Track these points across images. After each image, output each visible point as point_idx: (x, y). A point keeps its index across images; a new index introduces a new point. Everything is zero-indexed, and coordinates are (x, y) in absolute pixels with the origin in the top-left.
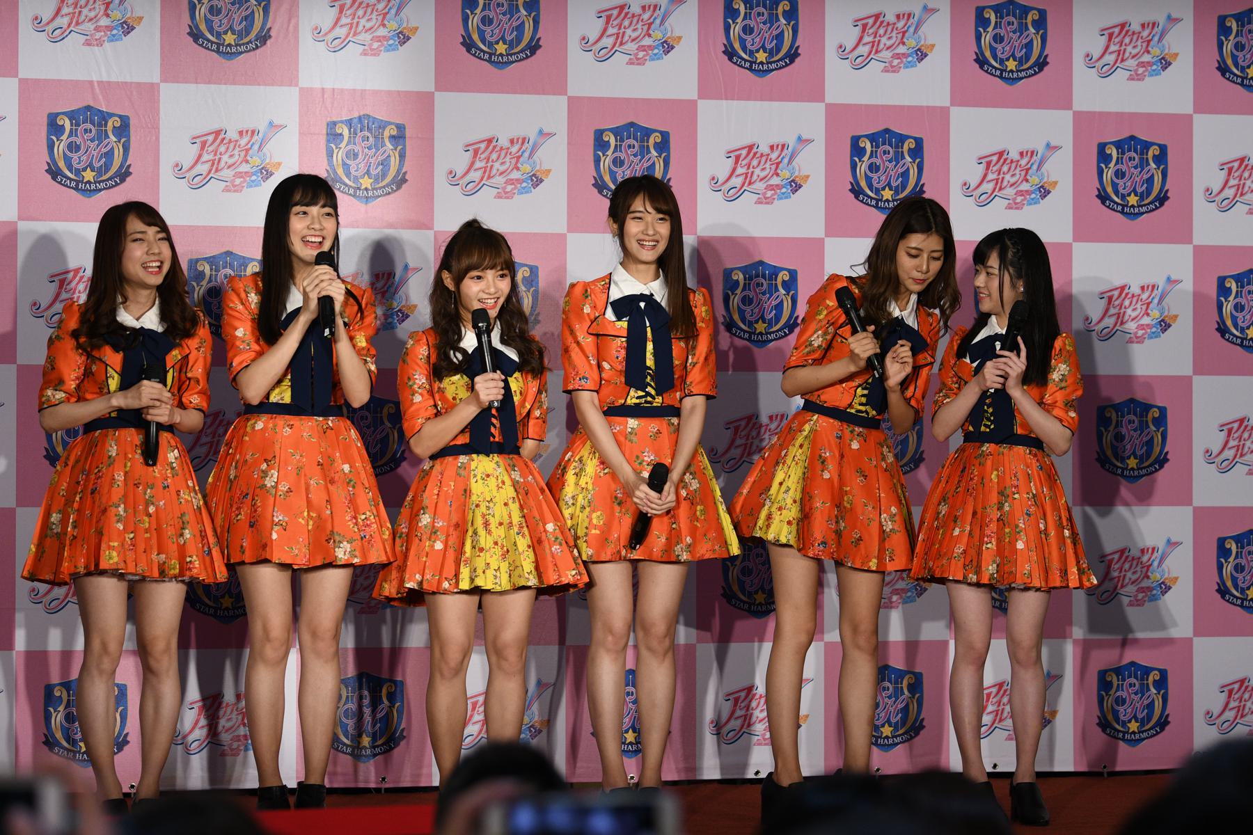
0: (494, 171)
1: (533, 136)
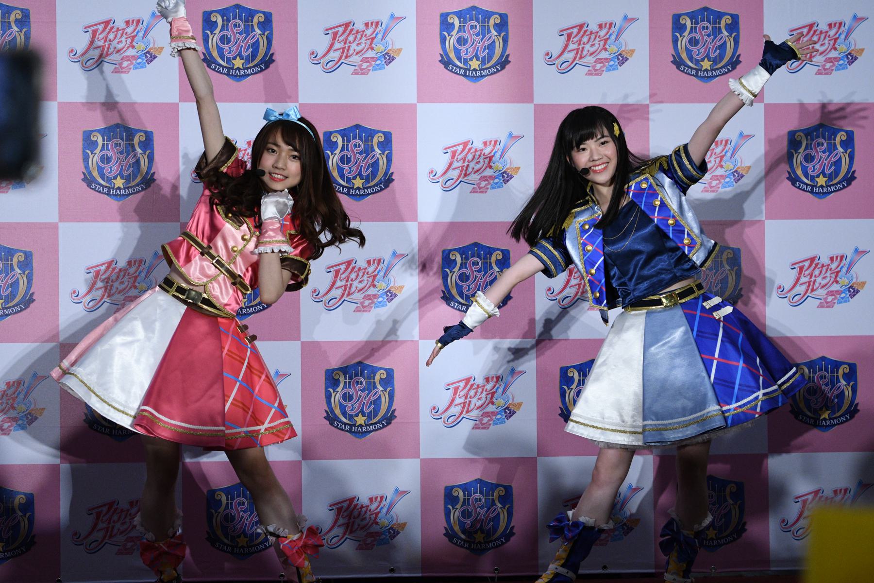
0: (585, 52)
1: (618, 21)
